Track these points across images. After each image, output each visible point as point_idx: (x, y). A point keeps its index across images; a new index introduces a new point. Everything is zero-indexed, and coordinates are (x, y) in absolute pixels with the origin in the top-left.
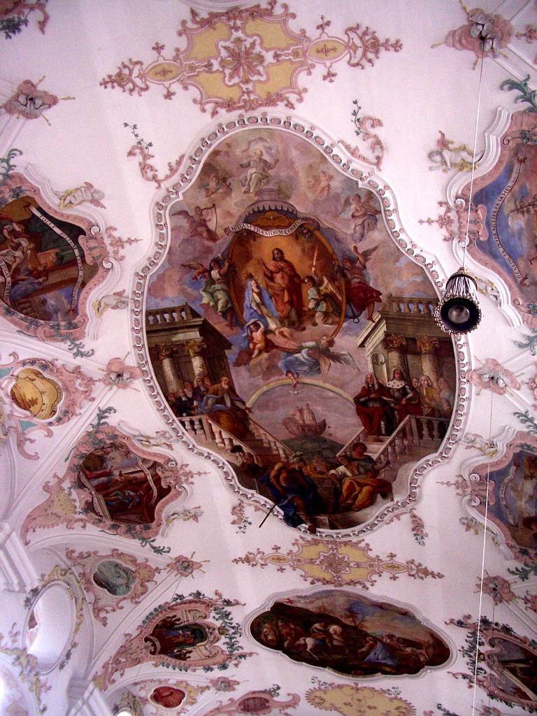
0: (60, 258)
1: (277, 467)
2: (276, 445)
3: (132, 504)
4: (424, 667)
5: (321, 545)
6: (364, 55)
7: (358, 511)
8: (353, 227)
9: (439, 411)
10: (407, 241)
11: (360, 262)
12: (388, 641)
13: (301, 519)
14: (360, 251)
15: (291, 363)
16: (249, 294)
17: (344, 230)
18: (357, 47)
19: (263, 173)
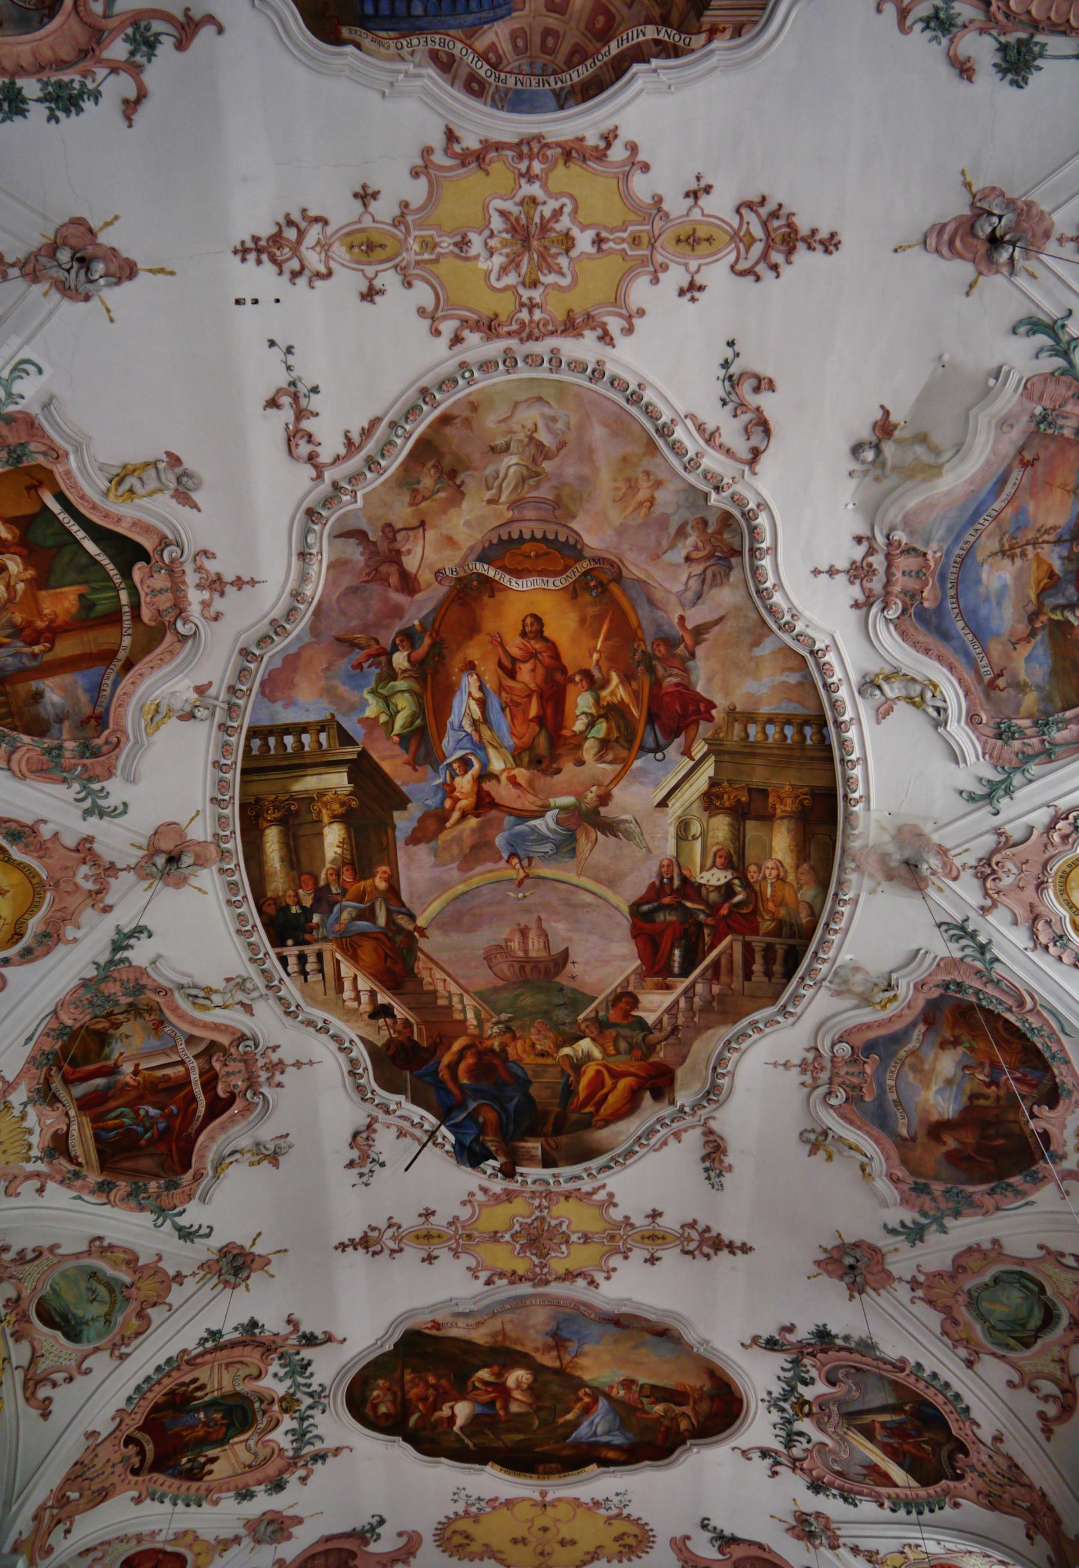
1: (456, 1046)
2: (462, 1002)
3: (148, 1135)
4: (685, 1443)
5: (518, 1201)
6: (765, 256)
7: (601, 1128)
9: (791, 925)
10: (784, 606)
11: (686, 647)
12: (622, 1393)
13: (487, 1149)
14: (690, 625)
15: (522, 837)
16: (461, 700)
17: (667, 585)
18: (753, 240)
19: (531, 467)
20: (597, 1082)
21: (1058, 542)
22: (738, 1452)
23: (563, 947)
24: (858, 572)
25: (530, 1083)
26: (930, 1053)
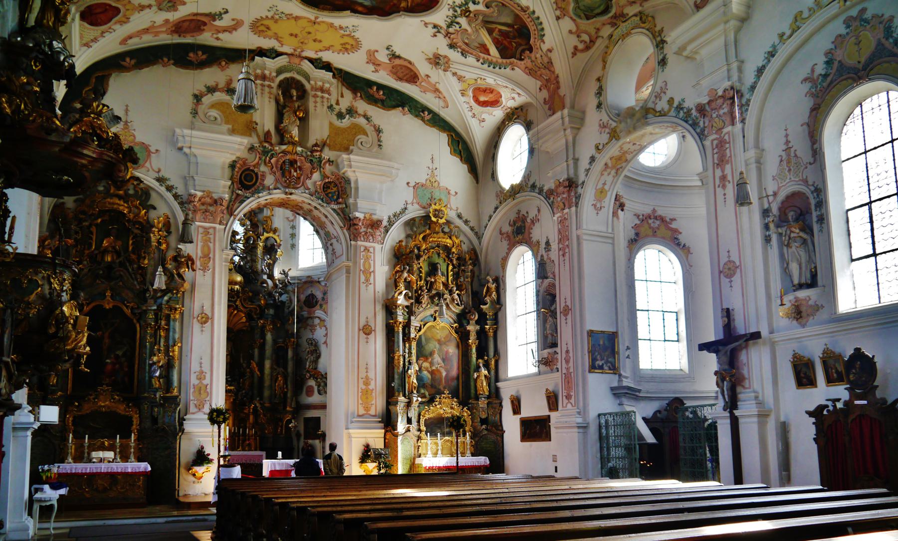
4: (399, 12)
22: (423, 23)
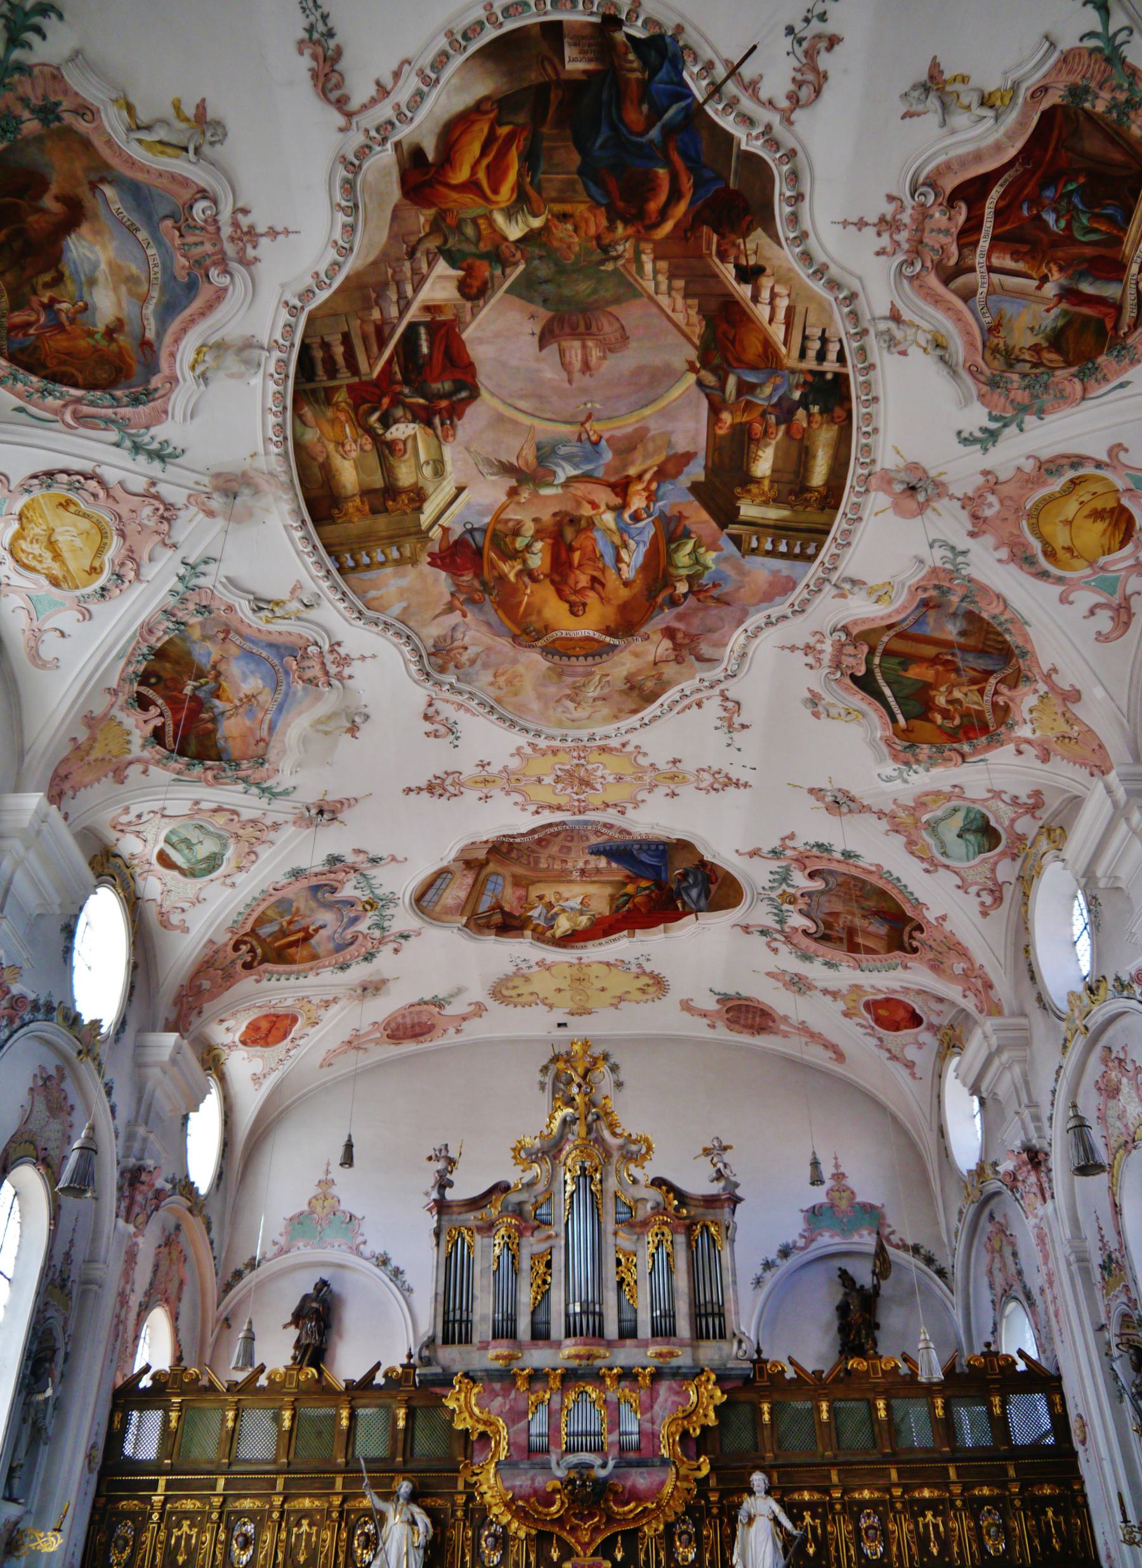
0: (905, 665)
1: (668, 227)
2: (657, 285)
3: (1071, 187)
8: (467, 639)
9: (317, 402)
13: (641, 56)
14: (458, 613)
15: (587, 459)
20: (496, 175)
21: (223, 713)
23: (545, 351)
24: (346, 661)
25: (580, 172)
26: (129, 309)
